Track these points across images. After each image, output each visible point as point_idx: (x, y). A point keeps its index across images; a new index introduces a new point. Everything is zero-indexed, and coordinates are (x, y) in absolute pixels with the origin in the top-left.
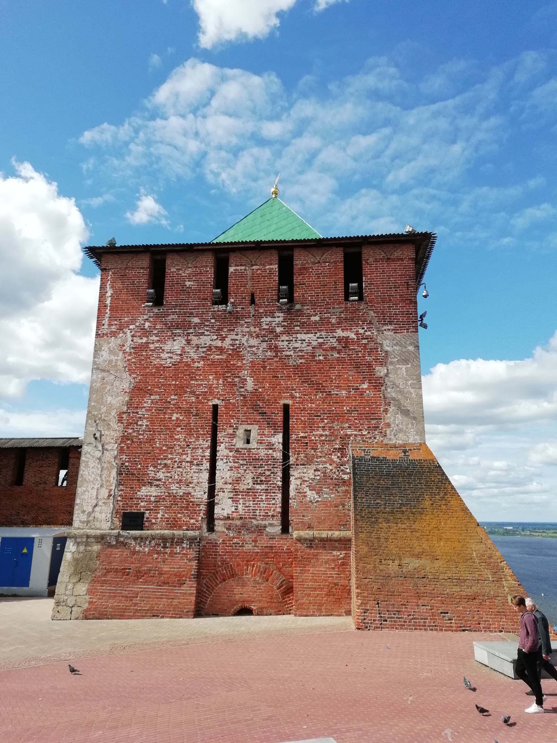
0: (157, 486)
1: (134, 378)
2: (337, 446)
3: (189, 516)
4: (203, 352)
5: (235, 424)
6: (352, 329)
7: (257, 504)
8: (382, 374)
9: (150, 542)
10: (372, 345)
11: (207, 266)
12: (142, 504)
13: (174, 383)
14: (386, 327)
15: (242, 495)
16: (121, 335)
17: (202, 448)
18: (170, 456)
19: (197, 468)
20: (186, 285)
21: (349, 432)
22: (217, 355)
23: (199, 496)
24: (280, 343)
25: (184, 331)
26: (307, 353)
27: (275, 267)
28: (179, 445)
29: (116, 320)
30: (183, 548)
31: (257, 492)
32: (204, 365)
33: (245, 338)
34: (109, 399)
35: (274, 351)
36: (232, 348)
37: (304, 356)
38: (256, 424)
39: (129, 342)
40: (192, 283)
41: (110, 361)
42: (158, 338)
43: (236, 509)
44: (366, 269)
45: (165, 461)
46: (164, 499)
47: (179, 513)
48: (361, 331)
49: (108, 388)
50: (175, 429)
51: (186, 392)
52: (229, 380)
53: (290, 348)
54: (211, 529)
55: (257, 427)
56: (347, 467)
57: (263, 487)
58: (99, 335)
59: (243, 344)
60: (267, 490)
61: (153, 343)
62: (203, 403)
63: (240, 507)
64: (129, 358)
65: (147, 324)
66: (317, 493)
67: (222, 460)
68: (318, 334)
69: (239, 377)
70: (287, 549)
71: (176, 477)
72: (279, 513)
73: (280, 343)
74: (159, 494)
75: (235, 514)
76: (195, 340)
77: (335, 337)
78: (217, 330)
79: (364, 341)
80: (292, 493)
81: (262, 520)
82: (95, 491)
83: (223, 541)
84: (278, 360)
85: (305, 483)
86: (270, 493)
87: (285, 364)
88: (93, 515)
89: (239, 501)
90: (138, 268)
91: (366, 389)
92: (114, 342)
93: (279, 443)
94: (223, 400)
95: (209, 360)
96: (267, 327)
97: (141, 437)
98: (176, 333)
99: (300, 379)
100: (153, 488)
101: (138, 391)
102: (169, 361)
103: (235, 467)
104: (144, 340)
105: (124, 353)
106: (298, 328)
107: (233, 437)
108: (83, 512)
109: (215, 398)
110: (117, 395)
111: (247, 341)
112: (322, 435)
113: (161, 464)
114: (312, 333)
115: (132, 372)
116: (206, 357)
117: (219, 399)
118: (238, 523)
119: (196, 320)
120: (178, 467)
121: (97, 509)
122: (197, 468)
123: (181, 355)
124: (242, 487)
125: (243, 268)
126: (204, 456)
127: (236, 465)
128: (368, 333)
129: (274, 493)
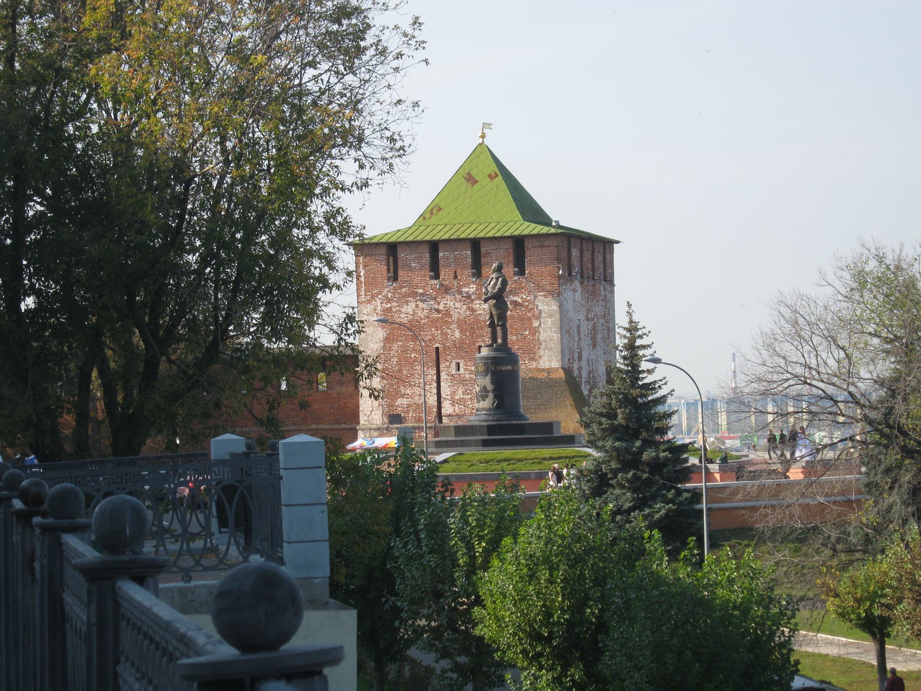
10: (531, 306)
27: (469, 252)
39: (379, 307)
44: (528, 253)
54: (440, 421)
63: (457, 408)
76: (421, 305)
79: (526, 304)
92: (370, 307)
101: (388, 340)
104: (389, 305)
110: (376, 343)
124: (457, 397)
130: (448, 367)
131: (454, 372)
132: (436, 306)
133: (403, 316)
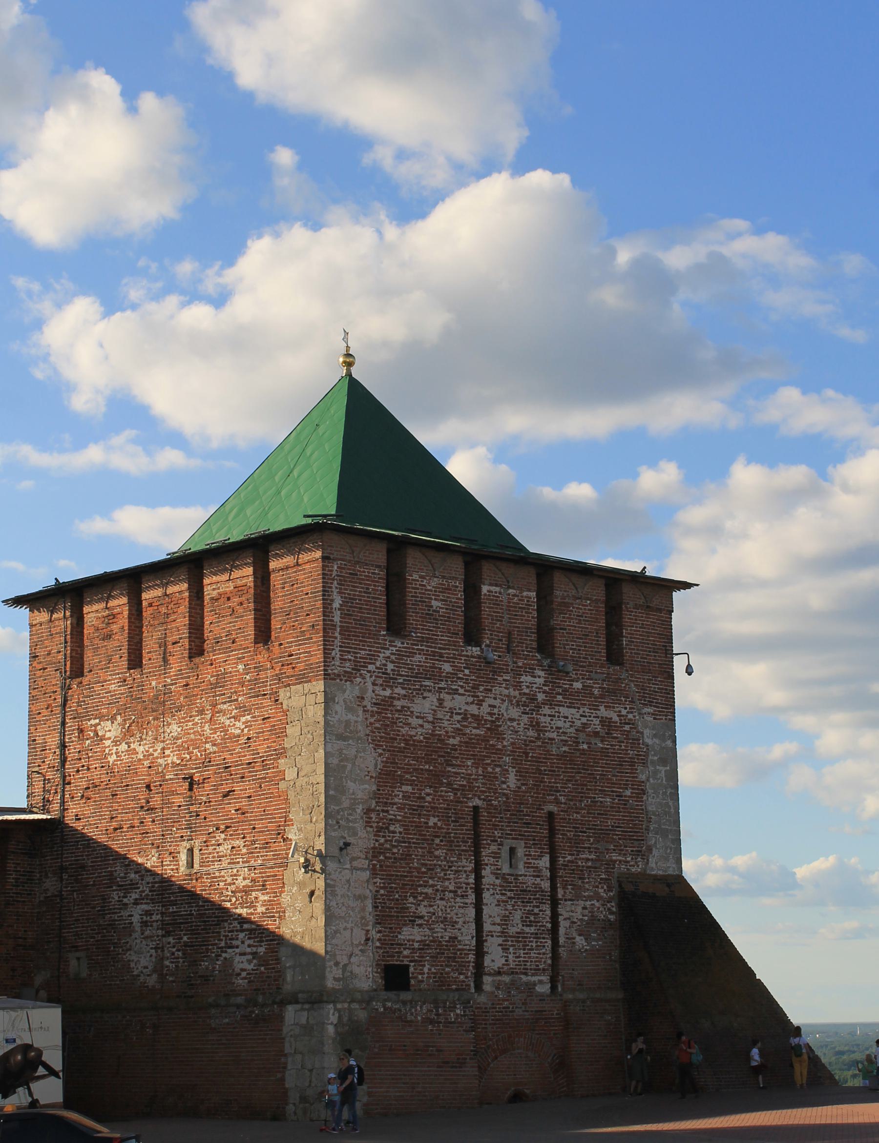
0: (420, 925)
1: (380, 755)
2: (603, 876)
3: (457, 970)
4: (458, 722)
5: (499, 837)
6: (614, 707)
7: (527, 954)
8: (643, 777)
9: (421, 1007)
11: (456, 579)
12: (406, 953)
13: (427, 767)
14: (646, 710)
15: (512, 941)
16: (358, 680)
17: (465, 872)
18: (431, 882)
19: (462, 901)
20: (432, 607)
21: (615, 856)
22: (474, 728)
23: (467, 942)
24: (542, 719)
25: (435, 683)
26: (570, 737)
28: (440, 866)
29: (349, 652)
30: (457, 1015)
31: (526, 937)
32: (460, 742)
33: (504, 706)
34: (350, 784)
35: (537, 730)
36: (490, 719)
37: (566, 741)
38: (521, 839)
40: (439, 604)
41: (348, 723)
42: (403, 692)
43: (506, 961)
45: (426, 890)
46: (428, 945)
47: (447, 966)
48: (624, 712)
49: (349, 768)
50: (433, 840)
51: (442, 784)
52: (490, 770)
53: (552, 728)
54: (479, 987)
55: (522, 843)
56: (613, 904)
57: (532, 930)
58: (329, 675)
59: (503, 715)
60: (536, 934)
61: (399, 699)
62: (461, 802)
63: (511, 956)
64: (372, 720)
65: (390, 667)
66: (586, 939)
67: (488, 889)
68: (582, 710)
69: (500, 766)
70: (557, 1014)
71: (440, 914)
72: (549, 965)
73: (542, 719)
74: (423, 938)
75: (506, 968)
77: (598, 717)
78: (473, 688)
79: (627, 728)
80: (562, 940)
81: (533, 975)
82: (349, 932)
83: (493, 1004)
84: (540, 744)
85: (575, 925)
86: (540, 938)
87: (548, 751)
88: (349, 968)
89: (508, 949)
90: (372, 565)
91: (630, 797)
92: (350, 691)
93: (546, 868)
94: (484, 800)
95: (465, 734)
96: (527, 691)
97: (395, 850)
98: (426, 686)
99: (564, 776)
100: (416, 930)
101: (387, 777)
102: (420, 730)
103: (503, 901)
104: (388, 693)
105: (364, 711)
106: (560, 698)
107: (499, 857)
108: (337, 964)
109: (475, 795)
111: (507, 710)
112: (588, 860)
113: (421, 893)
114: (574, 708)
115: (376, 745)
116: (461, 730)
117: (480, 799)
118: (506, 979)
119: (447, 667)
120: (442, 899)
121: (353, 959)
122: (462, 901)
123: (433, 723)
124: (512, 930)
125: (498, 589)
126: (468, 884)
127: (504, 898)
128: (630, 716)
129: (544, 938)
130: (496, 855)
131: (506, 869)
132: (473, 709)
133: (414, 721)
